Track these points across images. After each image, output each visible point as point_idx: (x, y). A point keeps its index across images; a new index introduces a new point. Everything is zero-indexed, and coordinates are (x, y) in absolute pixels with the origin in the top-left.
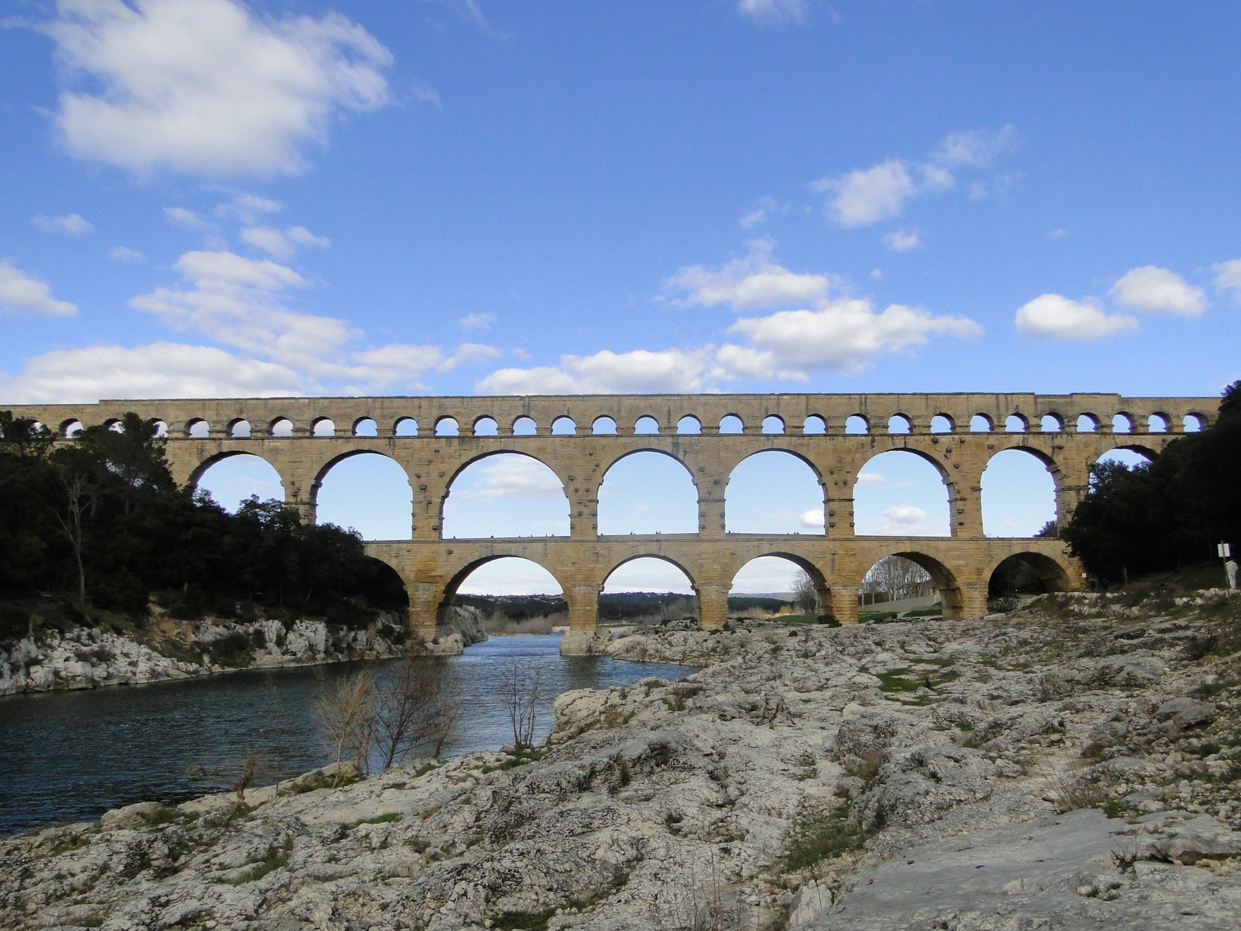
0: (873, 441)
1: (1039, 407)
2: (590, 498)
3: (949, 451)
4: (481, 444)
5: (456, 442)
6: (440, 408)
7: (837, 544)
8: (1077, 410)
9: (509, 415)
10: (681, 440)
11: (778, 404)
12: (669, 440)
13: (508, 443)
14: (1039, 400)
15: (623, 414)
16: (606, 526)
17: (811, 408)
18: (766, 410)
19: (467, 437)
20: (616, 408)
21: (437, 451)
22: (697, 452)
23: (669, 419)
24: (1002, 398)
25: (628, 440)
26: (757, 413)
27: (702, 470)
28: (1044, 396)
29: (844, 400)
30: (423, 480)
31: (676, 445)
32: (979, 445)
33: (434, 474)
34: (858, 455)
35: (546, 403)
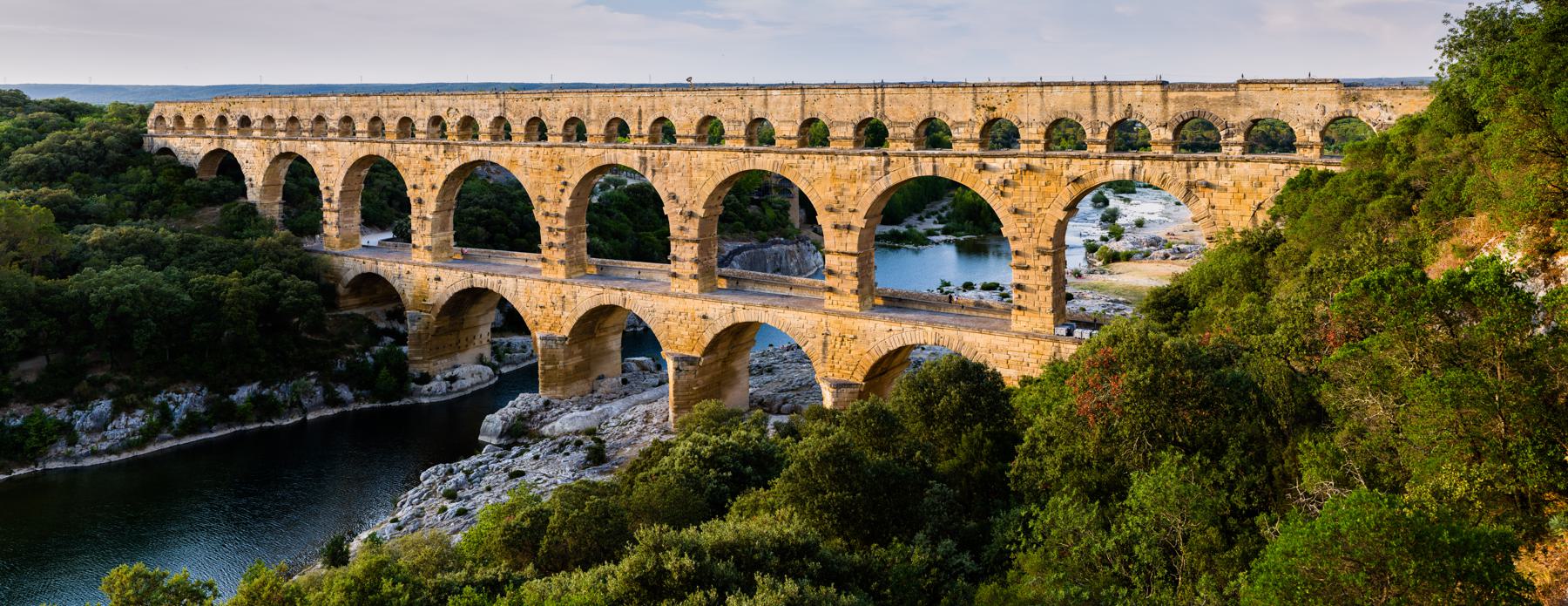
0: (888, 164)
1: (1172, 107)
6: (432, 106)
7: (832, 319)
8: (1242, 116)
11: (766, 103)
12: (636, 154)
14: (1172, 95)
15: (593, 116)
17: (808, 108)
18: (751, 112)
21: (428, 159)
24: (1102, 92)
26: (740, 117)
28: (1181, 87)
29: (852, 96)
31: (644, 160)
33: (427, 185)
34: (866, 186)
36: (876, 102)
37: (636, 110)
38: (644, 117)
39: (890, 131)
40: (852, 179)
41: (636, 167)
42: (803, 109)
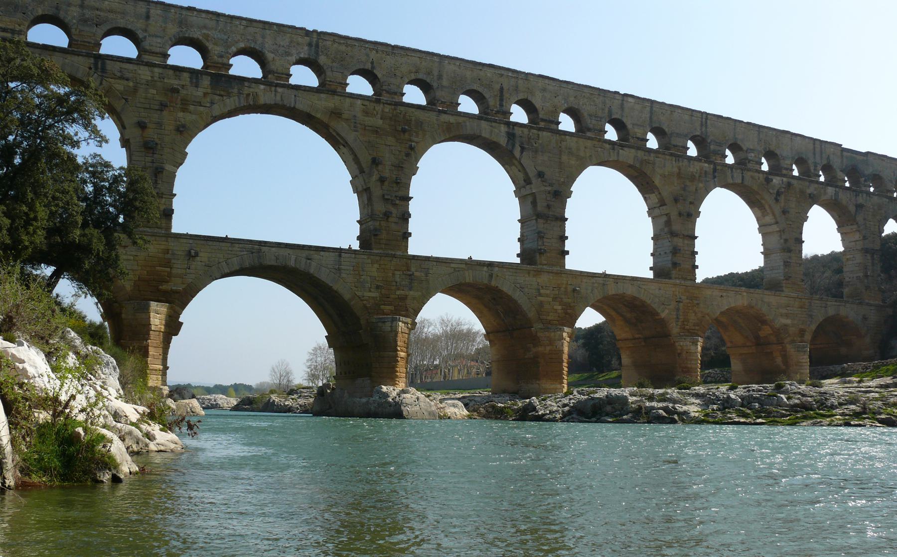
0: (715, 170)
1: (845, 160)
2: (400, 194)
3: (778, 194)
4: (246, 91)
5: (206, 81)
9: (288, 54)
10: (518, 132)
11: (622, 107)
12: (503, 129)
13: (290, 99)
14: (845, 154)
15: (445, 83)
16: (424, 241)
19: (216, 75)
20: (436, 73)
21: (175, 91)
22: (536, 151)
23: (501, 100)
25: (452, 119)
27: (540, 175)
30: (151, 133)
31: (511, 136)
32: (802, 192)
34: (701, 185)
35: (343, 48)
36: (702, 125)
37: (498, 87)
38: (506, 95)
39: (712, 147)
40: (692, 178)
41: (503, 141)
42: (651, 118)
